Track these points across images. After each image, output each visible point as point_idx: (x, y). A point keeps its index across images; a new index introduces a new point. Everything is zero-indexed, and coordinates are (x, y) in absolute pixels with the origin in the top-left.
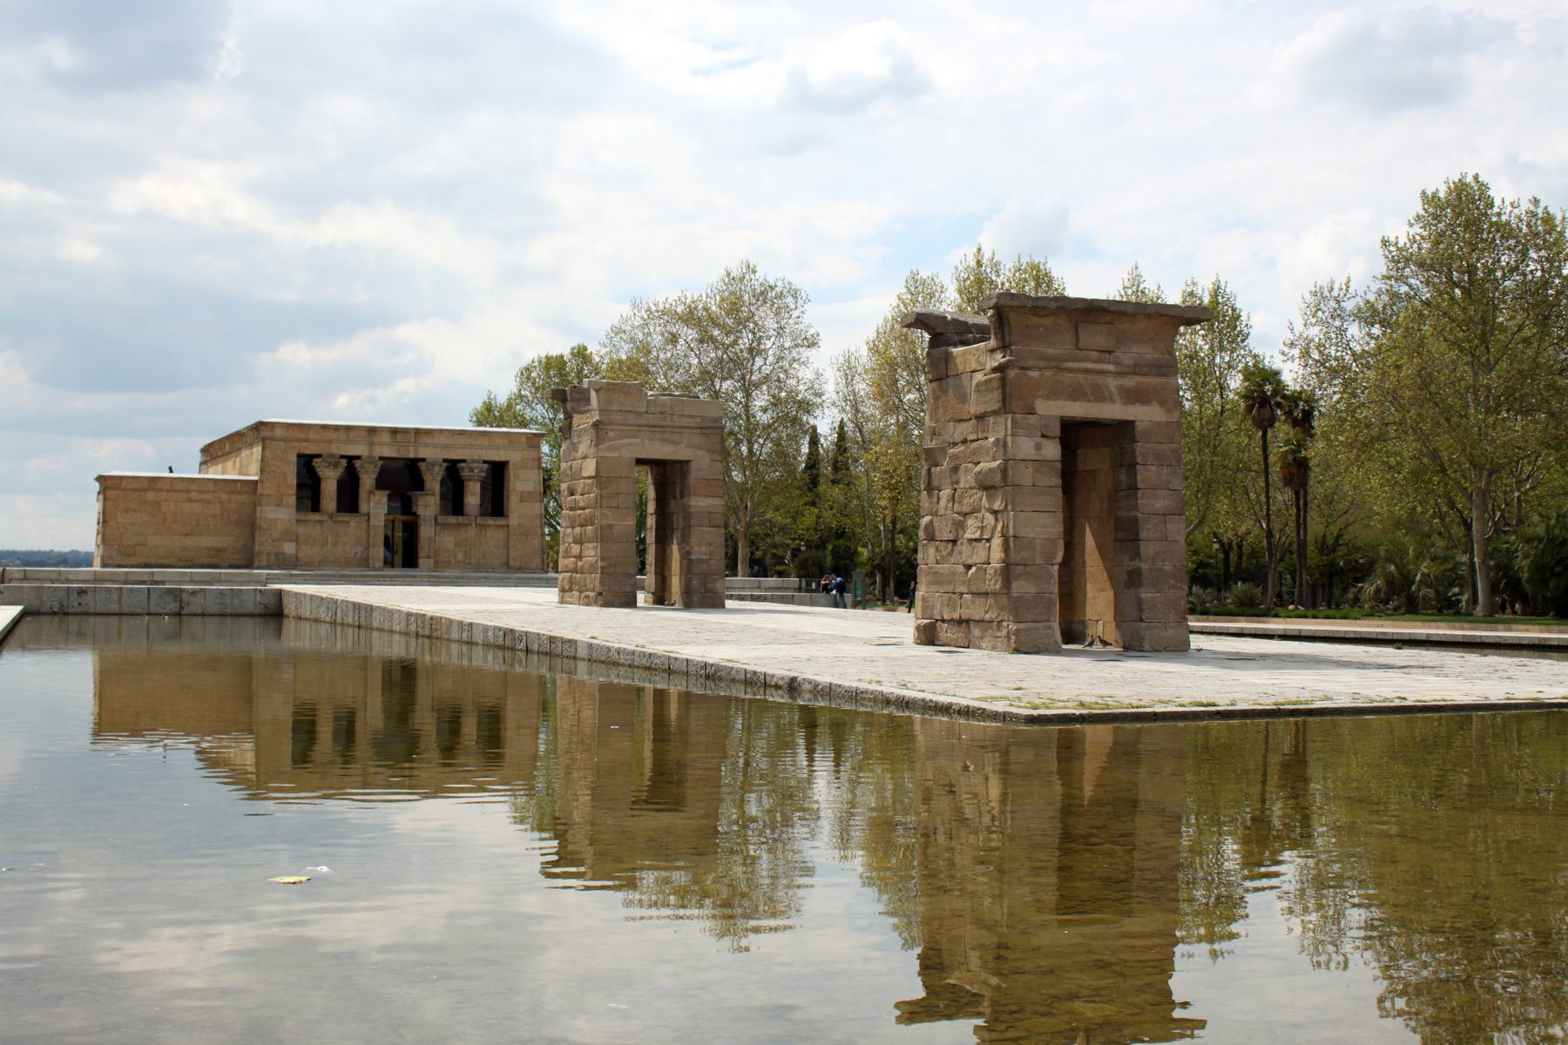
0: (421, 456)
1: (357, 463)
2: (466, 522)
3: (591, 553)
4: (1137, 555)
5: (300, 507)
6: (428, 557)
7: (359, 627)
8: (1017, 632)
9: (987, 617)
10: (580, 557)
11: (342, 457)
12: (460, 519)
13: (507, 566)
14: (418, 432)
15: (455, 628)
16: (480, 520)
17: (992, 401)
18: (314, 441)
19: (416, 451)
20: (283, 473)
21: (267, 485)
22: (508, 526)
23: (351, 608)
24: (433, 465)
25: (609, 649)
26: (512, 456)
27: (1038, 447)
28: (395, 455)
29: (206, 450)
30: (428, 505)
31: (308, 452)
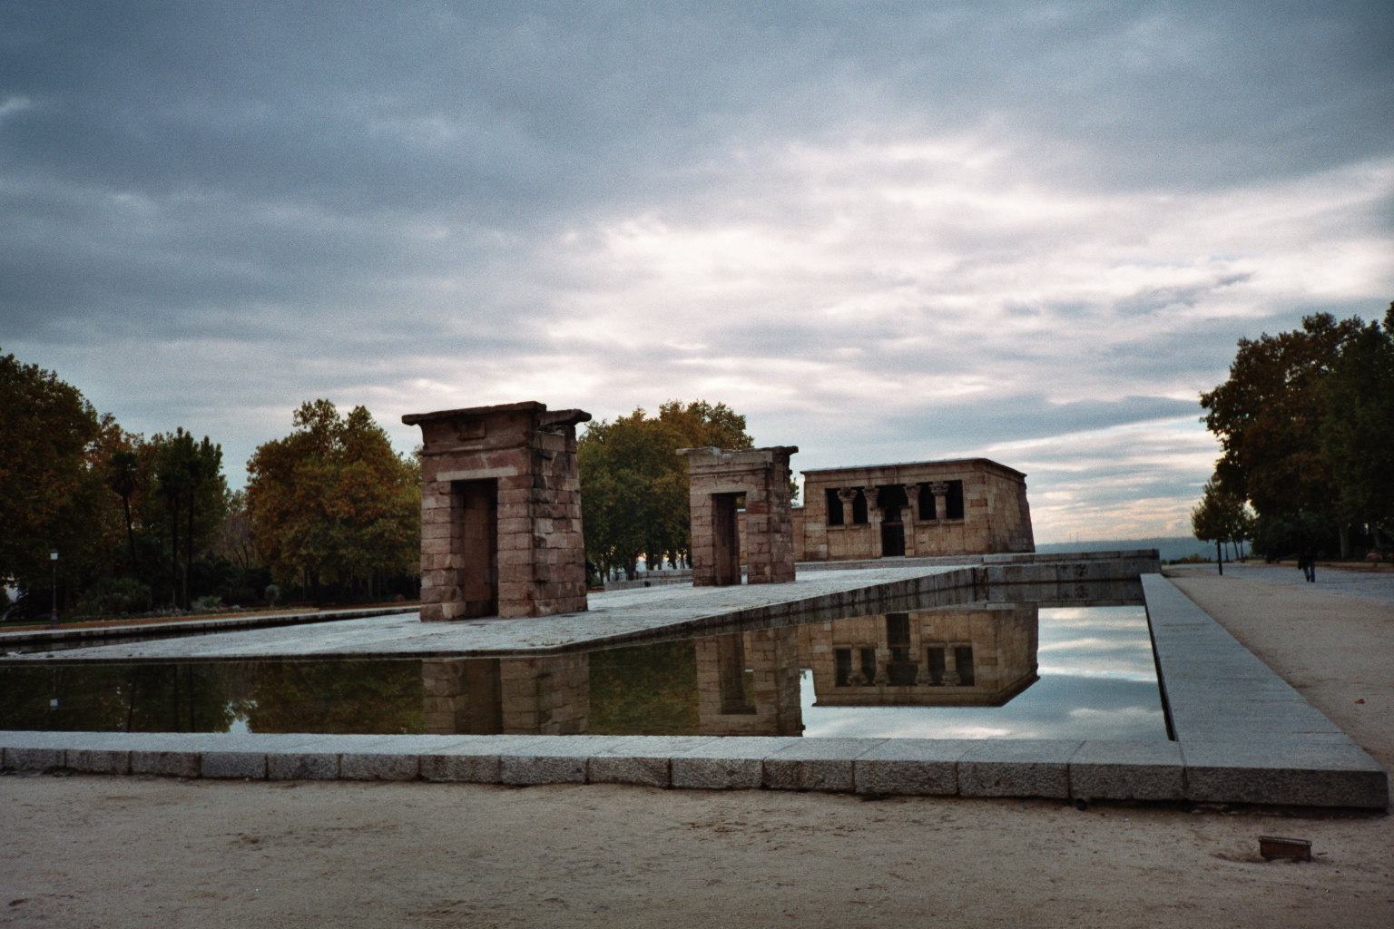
2: (934, 523)
6: (910, 548)
11: (853, 488)
14: (899, 468)
16: (942, 521)
18: (835, 481)
19: (898, 480)
20: (817, 501)
21: (808, 511)
22: (963, 524)
24: (909, 488)
26: (964, 476)
27: (437, 500)
28: (886, 484)
30: (907, 517)
31: (828, 487)
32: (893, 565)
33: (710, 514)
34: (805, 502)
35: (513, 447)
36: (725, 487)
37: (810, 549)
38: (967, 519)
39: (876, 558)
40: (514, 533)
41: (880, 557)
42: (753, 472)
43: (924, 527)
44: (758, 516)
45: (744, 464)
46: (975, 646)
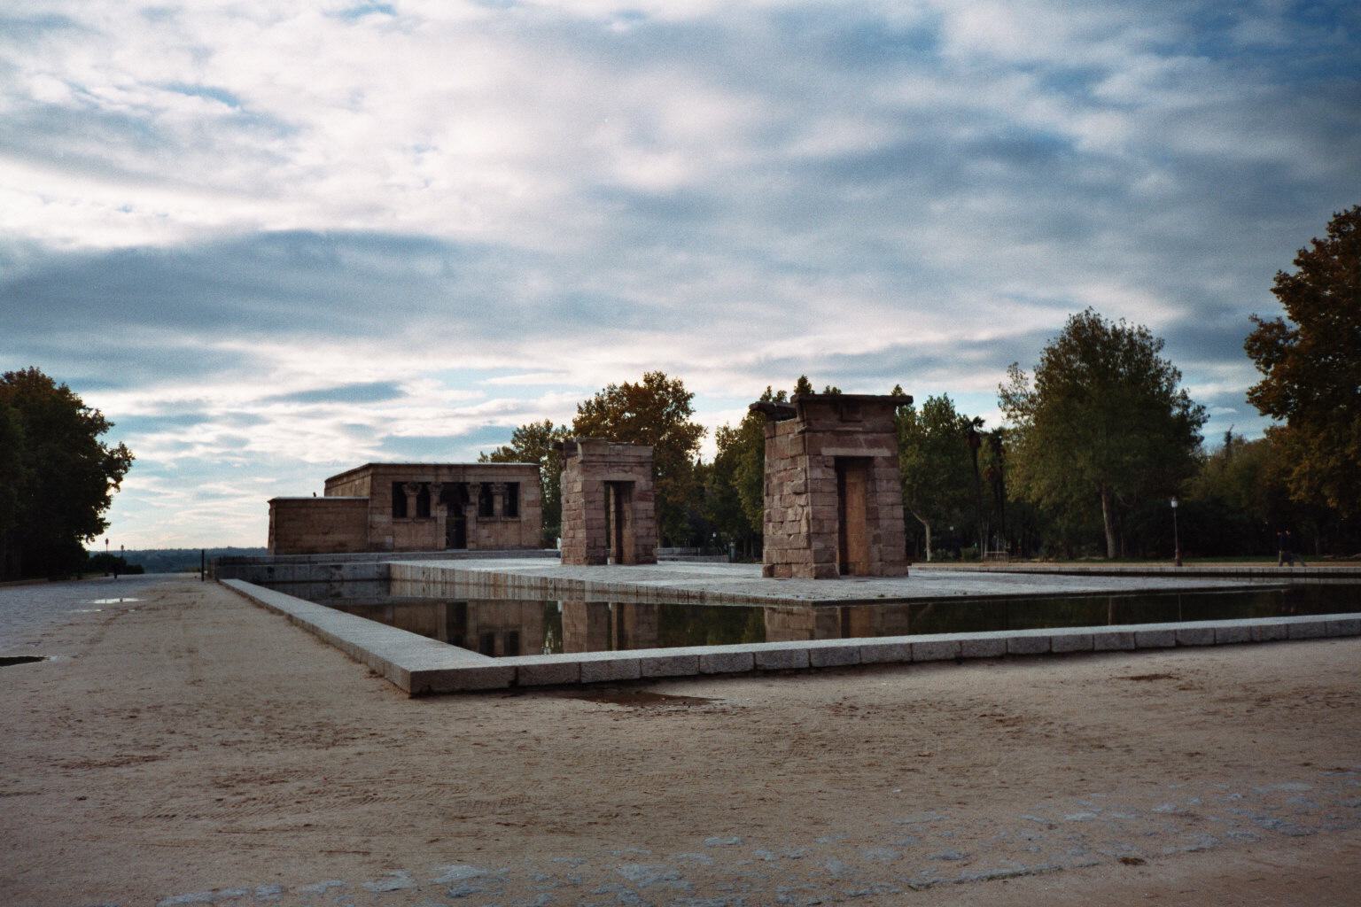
0: (467, 480)
1: (429, 487)
3: (581, 534)
4: (879, 527)
5: (395, 515)
6: (473, 542)
7: (446, 583)
8: (816, 568)
9: (800, 561)
10: (574, 537)
11: (419, 483)
12: (492, 519)
13: (521, 547)
15: (510, 579)
17: (800, 449)
18: (403, 475)
23: (440, 572)
25: (603, 584)
27: (823, 471)
29: (329, 482)
30: (471, 513)
32: (453, 557)
33: (603, 499)
34: (372, 493)
35: (886, 432)
36: (617, 476)
37: (376, 540)
38: (524, 518)
39: (440, 550)
40: (892, 505)
41: (445, 549)
42: (641, 464)
43: (486, 523)
44: (647, 504)
45: (633, 456)
46: (525, 629)
